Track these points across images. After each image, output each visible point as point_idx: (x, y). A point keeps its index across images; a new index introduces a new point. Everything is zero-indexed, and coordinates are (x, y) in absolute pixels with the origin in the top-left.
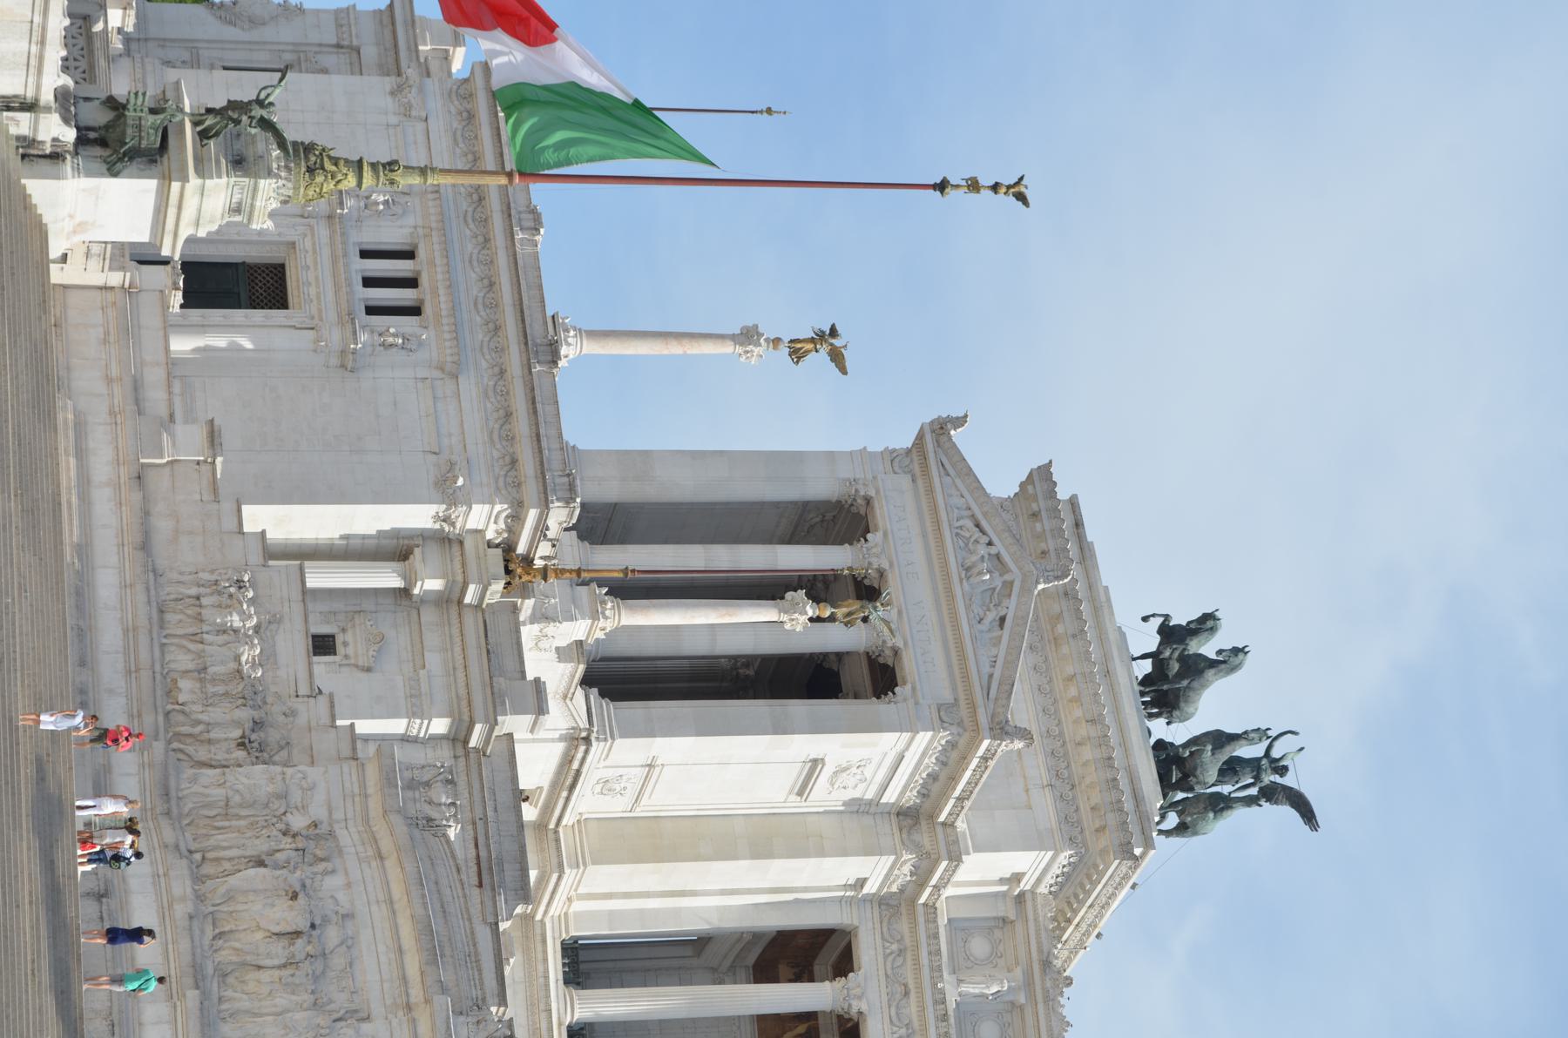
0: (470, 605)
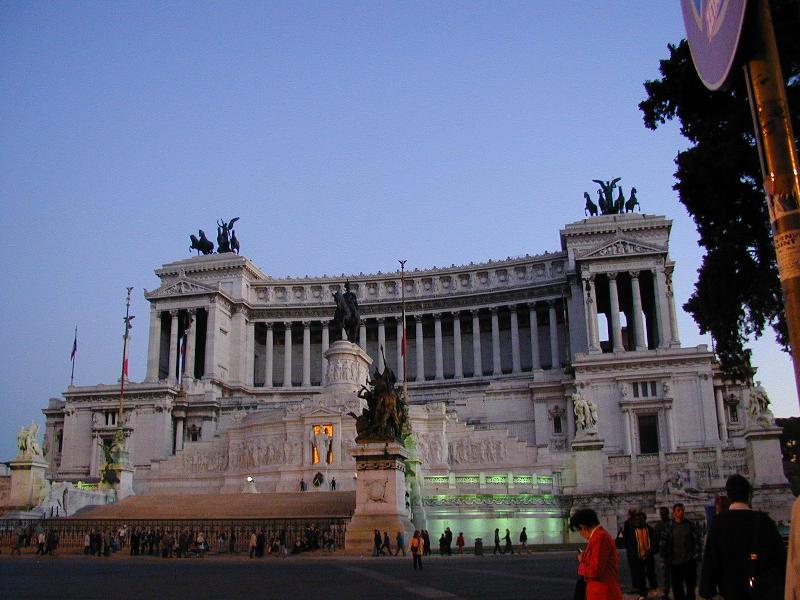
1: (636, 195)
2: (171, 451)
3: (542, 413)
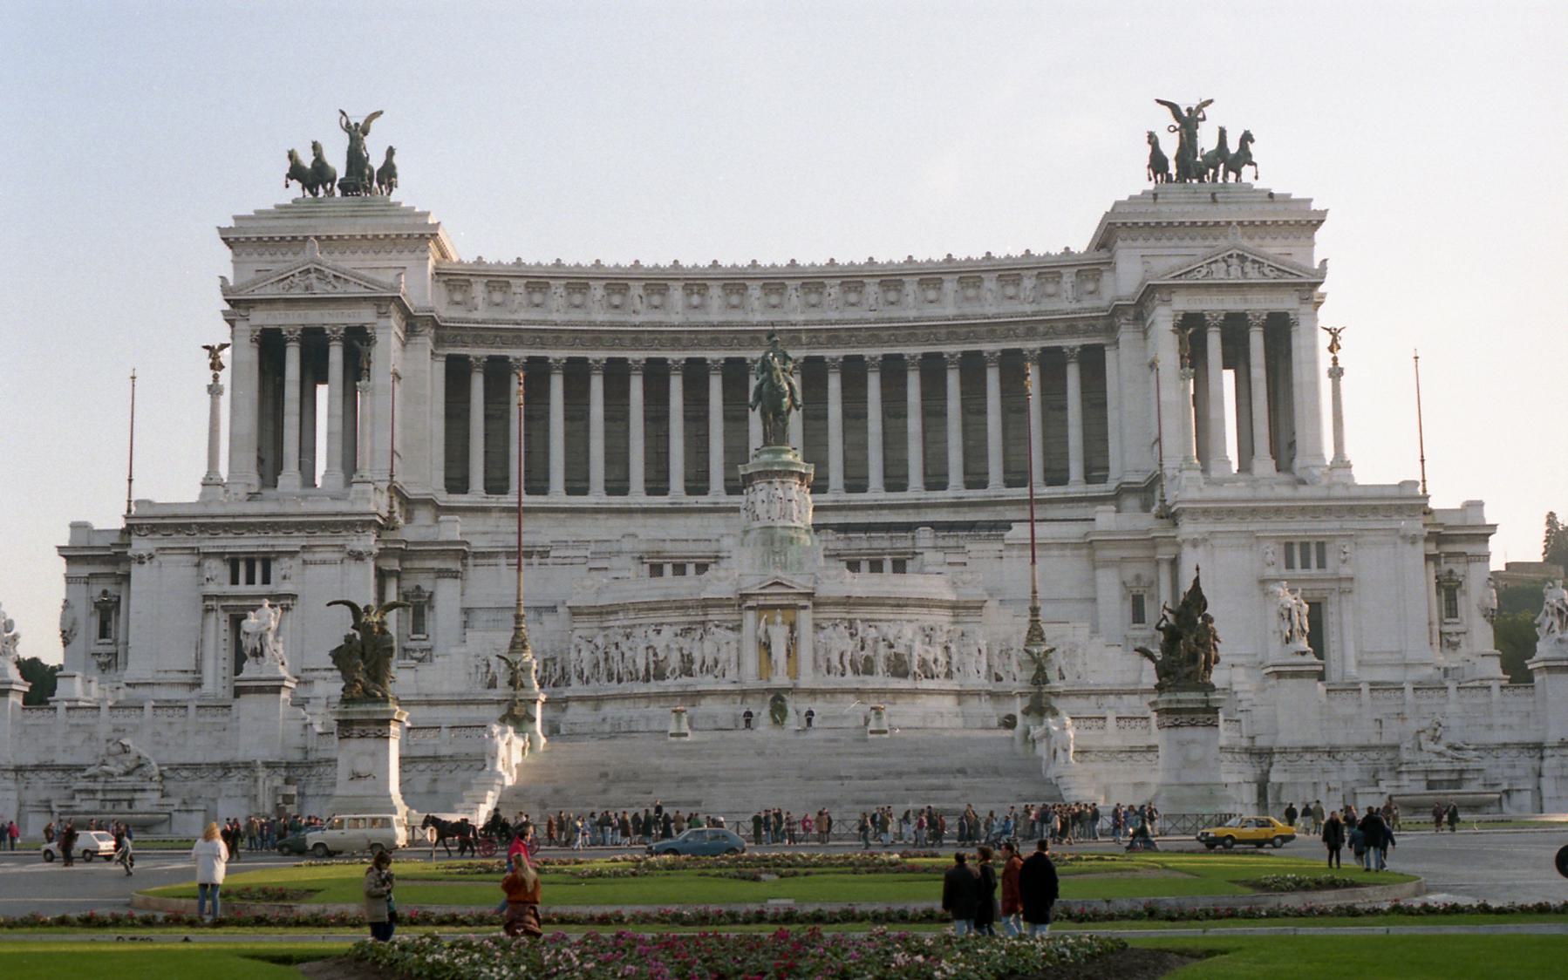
1: (1252, 147)
3: (1110, 587)
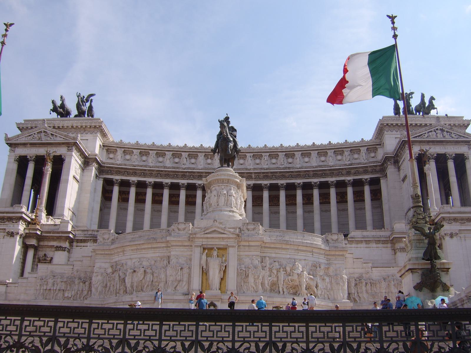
0: (41, 234)
2: (19, 274)
